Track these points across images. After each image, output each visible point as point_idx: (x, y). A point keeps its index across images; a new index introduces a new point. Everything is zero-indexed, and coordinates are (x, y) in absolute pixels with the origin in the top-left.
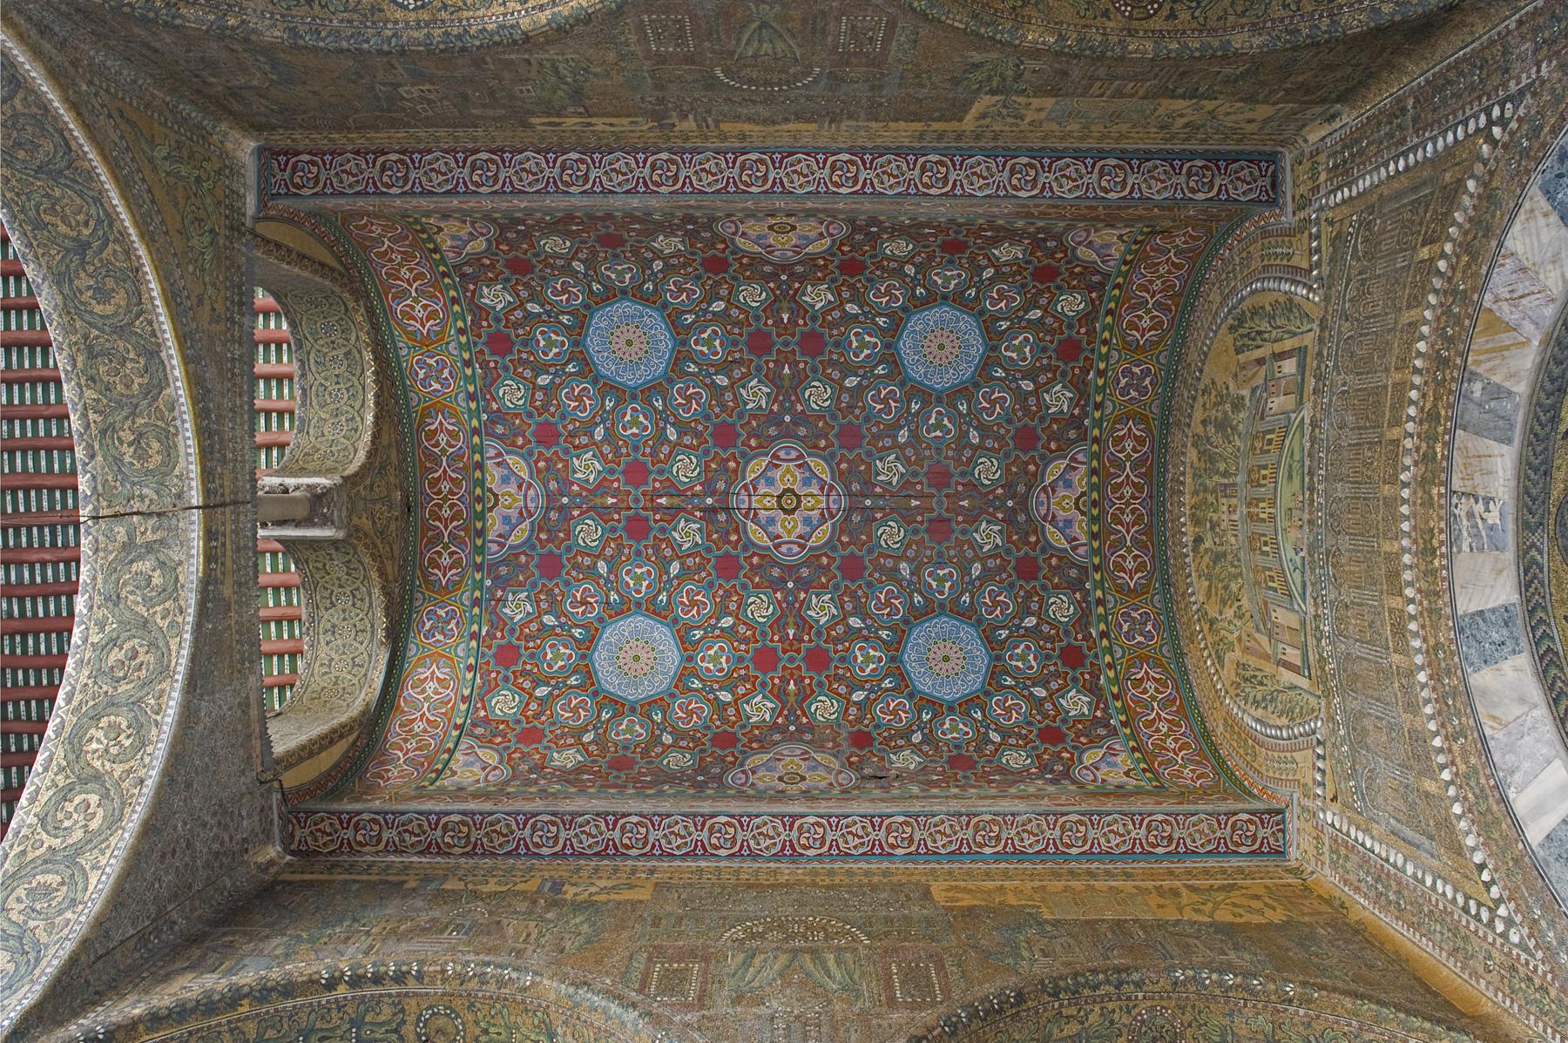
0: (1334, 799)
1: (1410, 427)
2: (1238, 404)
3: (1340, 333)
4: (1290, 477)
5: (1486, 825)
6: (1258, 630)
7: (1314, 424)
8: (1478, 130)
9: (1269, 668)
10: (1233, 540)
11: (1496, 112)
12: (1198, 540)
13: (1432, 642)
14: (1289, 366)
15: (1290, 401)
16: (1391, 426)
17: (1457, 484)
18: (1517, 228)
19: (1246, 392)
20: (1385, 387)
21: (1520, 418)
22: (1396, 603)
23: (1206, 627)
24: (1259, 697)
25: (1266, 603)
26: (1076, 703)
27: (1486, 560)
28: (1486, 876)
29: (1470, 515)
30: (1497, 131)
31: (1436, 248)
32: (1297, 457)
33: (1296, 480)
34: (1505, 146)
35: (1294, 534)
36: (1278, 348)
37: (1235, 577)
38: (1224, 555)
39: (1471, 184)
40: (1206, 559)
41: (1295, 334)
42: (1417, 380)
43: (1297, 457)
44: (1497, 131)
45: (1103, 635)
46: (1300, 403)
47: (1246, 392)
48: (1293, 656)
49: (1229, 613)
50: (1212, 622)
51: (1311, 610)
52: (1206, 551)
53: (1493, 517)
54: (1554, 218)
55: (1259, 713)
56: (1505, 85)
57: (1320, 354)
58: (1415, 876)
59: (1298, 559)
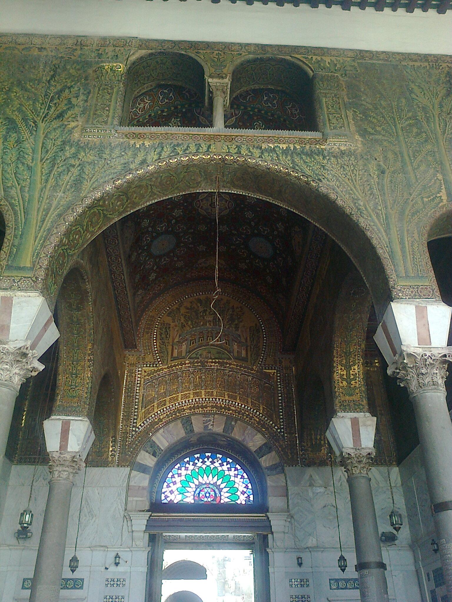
0: (145, 372)
1: (227, 401)
2: (237, 328)
3: (249, 376)
4: (218, 353)
5: (152, 424)
6: (180, 336)
7: (230, 364)
8: (281, 425)
9: (171, 340)
10: (202, 323)
11: (283, 430)
12: (200, 301)
13: (185, 408)
14: (244, 353)
15: (236, 354)
16: (228, 394)
17: (216, 416)
18: (260, 436)
19: (239, 333)
20: (236, 393)
21: (227, 435)
22: (192, 396)
23: (176, 306)
24: (163, 336)
25: (186, 340)
26: (153, 276)
27: (202, 426)
28: (142, 424)
29: (210, 420)
30: (279, 430)
31: (261, 412)
32: (223, 356)
33: (217, 356)
34: (276, 432)
35: (204, 354)
36: (249, 348)
37: (192, 324)
38: (197, 318)
39: (271, 422)
40: (196, 307)
41: (251, 357)
42: (237, 404)
43: (223, 356)
44: (279, 430)
45: (172, 274)
46: (235, 358)
47: (239, 333)
48: (175, 354)
49: (182, 320)
50: (178, 309)
51: (187, 362)
52: (198, 307)
53: (210, 427)
54: (260, 445)
55: (159, 336)
56: (286, 433)
57: (245, 368)
58: (136, 402)
59: (198, 356)
